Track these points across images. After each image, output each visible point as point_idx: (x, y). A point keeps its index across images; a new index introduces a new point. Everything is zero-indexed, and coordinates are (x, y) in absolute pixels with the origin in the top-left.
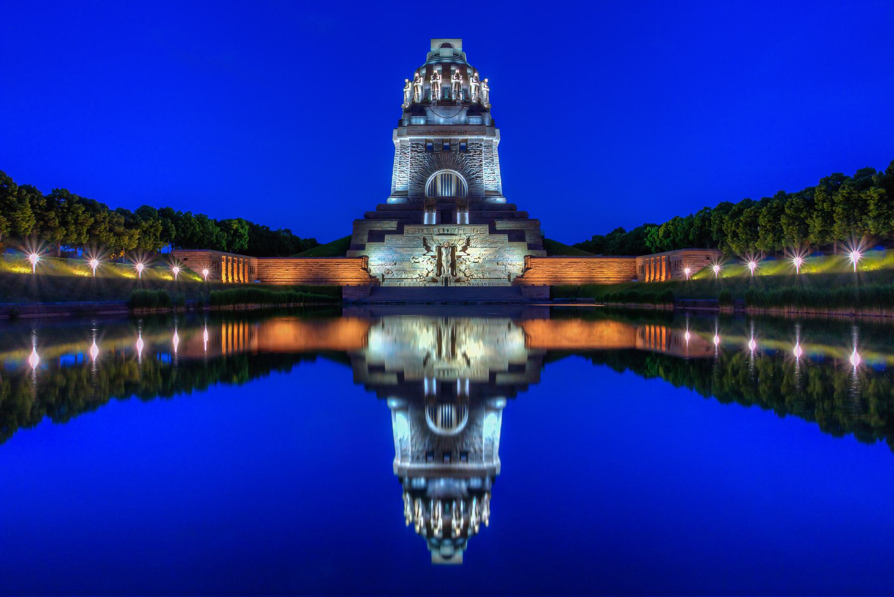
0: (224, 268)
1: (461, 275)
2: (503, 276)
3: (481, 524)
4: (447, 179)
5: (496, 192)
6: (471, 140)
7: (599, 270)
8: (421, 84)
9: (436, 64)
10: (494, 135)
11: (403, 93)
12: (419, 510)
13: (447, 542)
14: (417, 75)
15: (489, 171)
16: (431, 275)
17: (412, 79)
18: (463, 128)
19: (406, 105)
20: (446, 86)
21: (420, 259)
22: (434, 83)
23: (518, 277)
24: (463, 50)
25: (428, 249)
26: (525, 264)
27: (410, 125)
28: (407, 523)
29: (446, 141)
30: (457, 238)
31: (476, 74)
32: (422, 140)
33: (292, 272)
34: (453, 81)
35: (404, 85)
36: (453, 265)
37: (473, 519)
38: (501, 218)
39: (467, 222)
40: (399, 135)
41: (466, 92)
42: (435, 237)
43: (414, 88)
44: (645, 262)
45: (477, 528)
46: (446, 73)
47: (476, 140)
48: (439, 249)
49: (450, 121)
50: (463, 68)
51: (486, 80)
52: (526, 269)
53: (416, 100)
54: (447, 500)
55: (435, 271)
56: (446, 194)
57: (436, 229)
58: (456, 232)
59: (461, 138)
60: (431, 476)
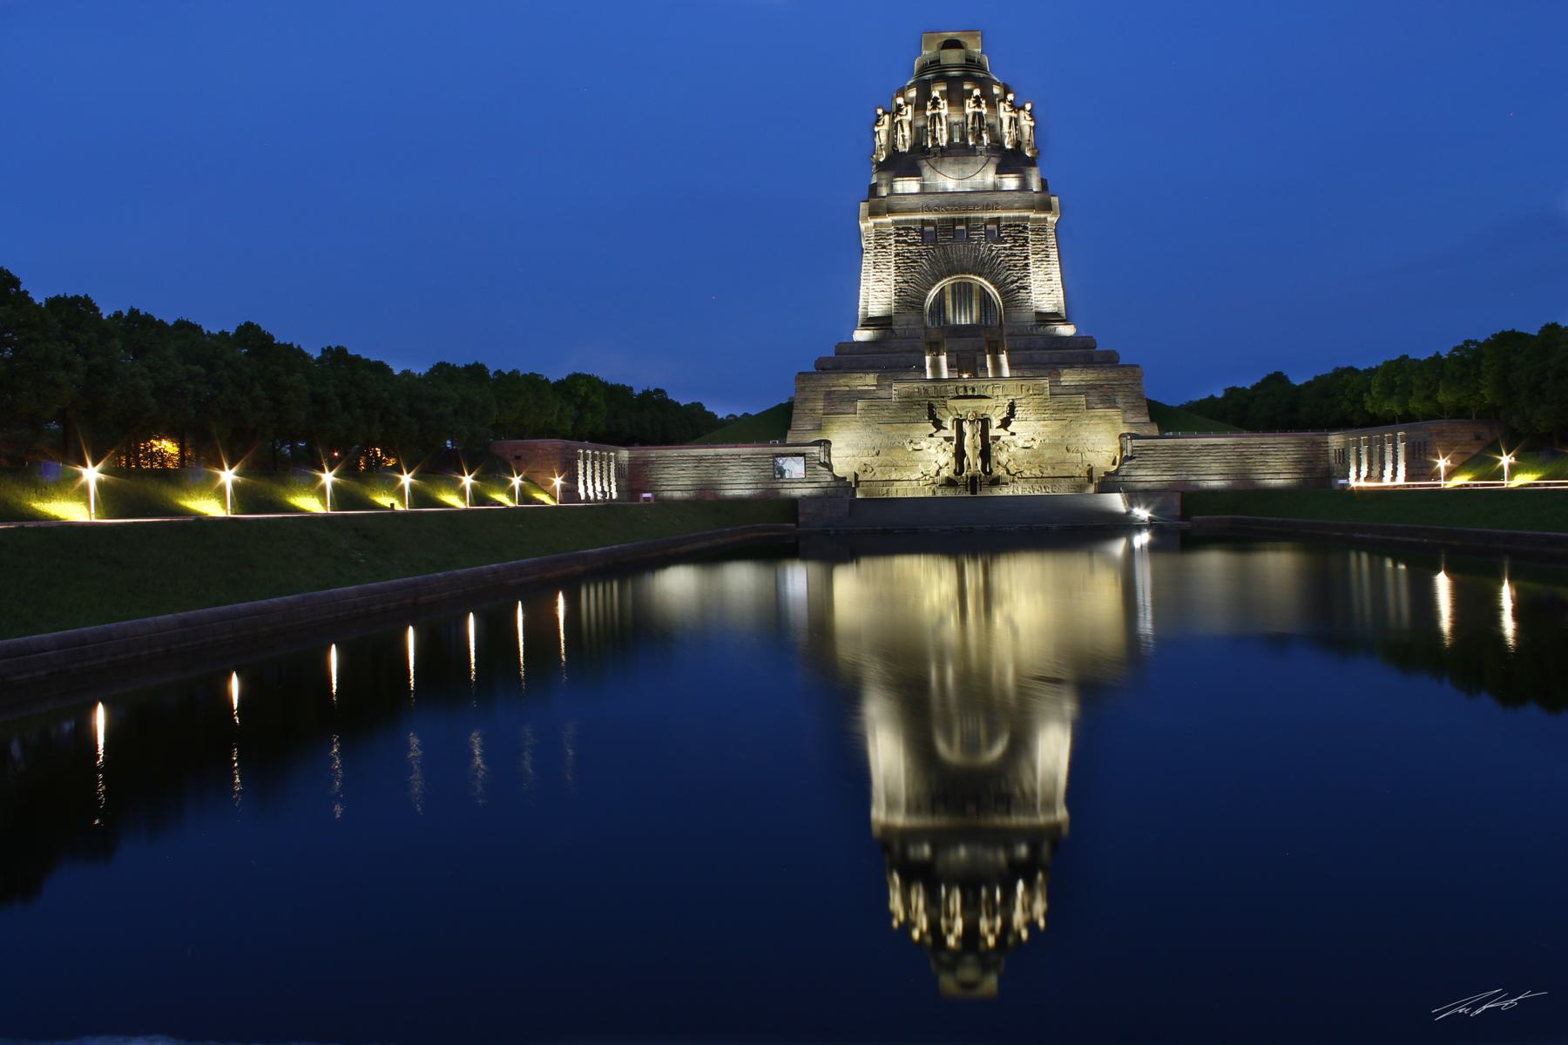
0: (581, 472)
1: (1000, 472)
2: (1077, 472)
3: (1031, 924)
6: (1007, 219)
12: (919, 901)
13: (970, 959)
15: (1041, 276)
16: (945, 473)
20: (956, 118)
21: (924, 444)
22: (934, 116)
23: (1108, 474)
25: (938, 425)
26: (1122, 449)
28: (895, 924)
29: (960, 221)
32: (915, 221)
33: (691, 472)
36: (985, 454)
37: (1018, 917)
38: (1070, 364)
39: (1006, 372)
40: (873, 213)
42: (951, 403)
43: (894, 127)
44: (1347, 443)
45: (1024, 934)
47: (1015, 219)
48: (959, 424)
49: (967, 186)
53: (901, 148)
54: (971, 884)
55: (953, 465)
56: (963, 320)
57: (951, 388)
58: (989, 393)
60: (941, 840)
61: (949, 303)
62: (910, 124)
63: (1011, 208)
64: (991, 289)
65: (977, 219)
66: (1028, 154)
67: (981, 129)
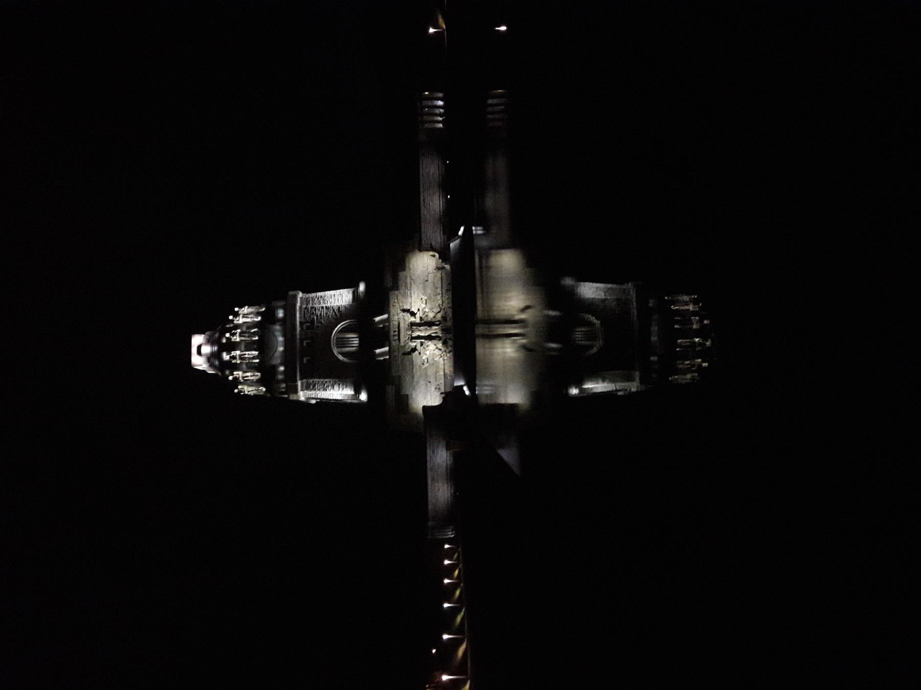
1: (439, 316)
2: (439, 275)
5: (354, 293)
8: (240, 373)
10: (295, 297)
15: (332, 300)
16: (440, 345)
20: (243, 347)
23: (440, 258)
25: (414, 350)
29: (301, 342)
30: (402, 321)
31: (231, 317)
34: (238, 340)
36: (430, 324)
37: (691, 308)
41: (249, 328)
42: (402, 344)
43: (246, 382)
47: (300, 313)
48: (413, 338)
49: (281, 339)
51: (236, 309)
52: (432, 249)
55: (435, 342)
56: (356, 342)
57: (394, 343)
58: (396, 323)
62: (244, 372)
63: (295, 315)
65: (300, 335)
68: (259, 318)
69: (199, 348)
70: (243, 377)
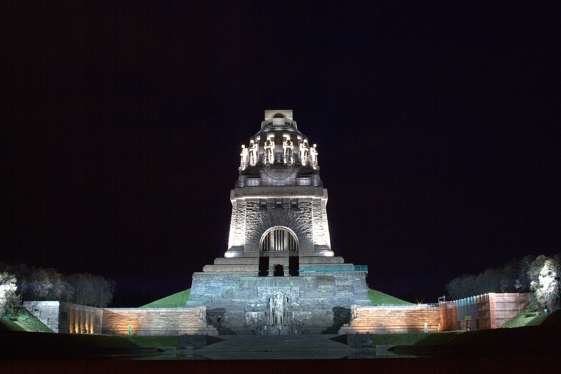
4: (279, 235)
7: (420, 318)
9: (270, 132)
10: (322, 195)
11: (239, 158)
14: (252, 141)
17: (248, 146)
18: (294, 188)
19: (243, 168)
20: (278, 151)
22: (268, 149)
24: (293, 120)
27: (246, 186)
29: (279, 200)
31: (305, 141)
32: (256, 200)
35: (241, 150)
40: (237, 196)
41: (297, 157)
46: (279, 141)
47: (305, 199)
49: (282, 183)
50: (293, 136)
51: (315, 146)
53: (251, 164)
59: (292, 197)
61: (272, 240)
63: (304, 194)
64: (293, 233)
66: (315, 168)
67: (290, 156)
68: (304, 164)
69: (281, 116)
70: (252, 151)
